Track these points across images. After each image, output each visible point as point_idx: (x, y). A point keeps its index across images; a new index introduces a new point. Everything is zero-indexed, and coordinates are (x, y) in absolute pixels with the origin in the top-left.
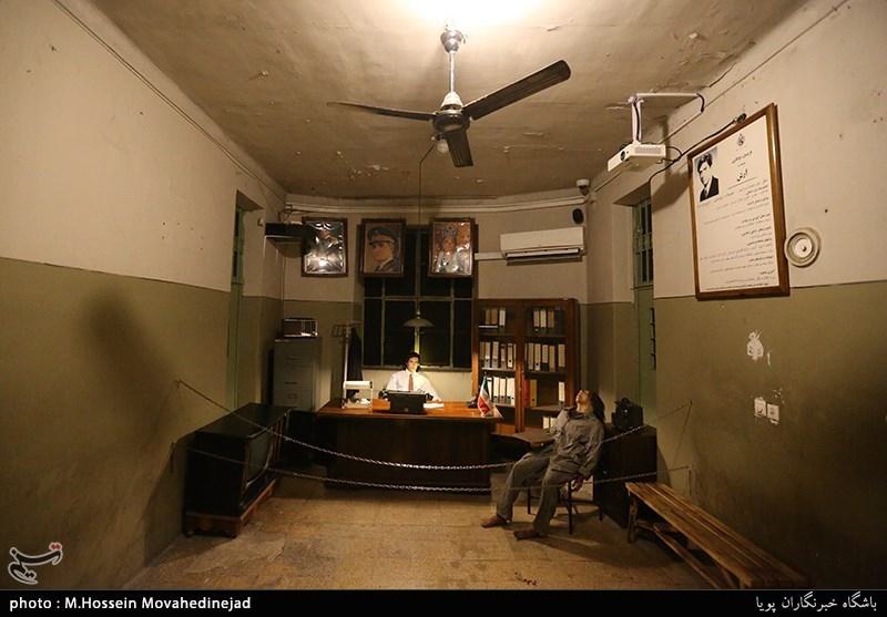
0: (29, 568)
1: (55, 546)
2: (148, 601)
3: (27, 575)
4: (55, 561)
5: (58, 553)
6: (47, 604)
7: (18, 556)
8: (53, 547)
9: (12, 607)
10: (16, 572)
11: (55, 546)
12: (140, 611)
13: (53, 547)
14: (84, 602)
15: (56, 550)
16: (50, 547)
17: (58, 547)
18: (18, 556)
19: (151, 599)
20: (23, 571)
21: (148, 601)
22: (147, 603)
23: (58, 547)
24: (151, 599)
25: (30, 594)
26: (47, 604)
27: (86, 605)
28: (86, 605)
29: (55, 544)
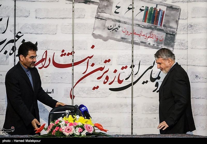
0: (7, 132)
1: (13, 128)
2: (27, 140)
3: (6, 134)
4: (13, 131)
5: (13, 129)
6: (10, 141)
7: (4, 130)
8: (12, 128)
9: (3, 142)
10: (4, 133)
11: (13, 128)
12: (25, 142)
13: (12, 128)
14: (14, 141)
15: (13, 128)
16: (11, 128)
17: (13, 128)
18: (4, 130)
19: (28, 140)
20: (5, 133)
21: (27, 140)
22: (27, 141)
23: (13, 128)
24: (28, 140)
25: (6, 139)
26: (10, 141)
27: (15, 141)
28: (15, 141)
29: (13, 127)
